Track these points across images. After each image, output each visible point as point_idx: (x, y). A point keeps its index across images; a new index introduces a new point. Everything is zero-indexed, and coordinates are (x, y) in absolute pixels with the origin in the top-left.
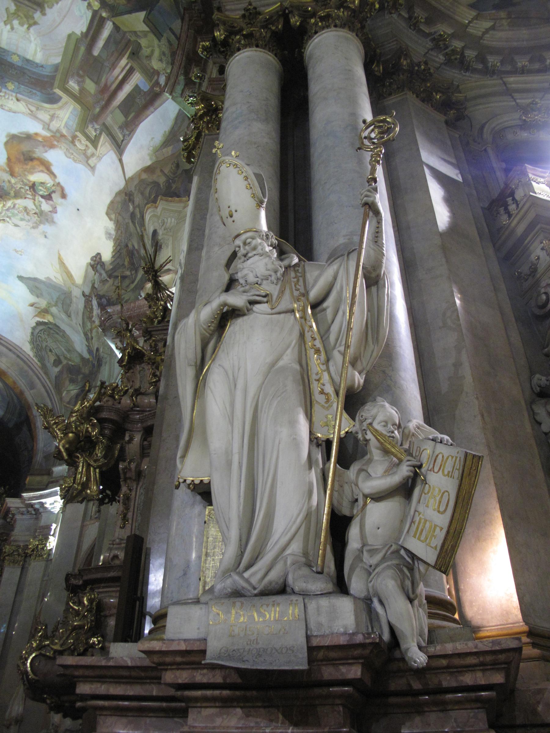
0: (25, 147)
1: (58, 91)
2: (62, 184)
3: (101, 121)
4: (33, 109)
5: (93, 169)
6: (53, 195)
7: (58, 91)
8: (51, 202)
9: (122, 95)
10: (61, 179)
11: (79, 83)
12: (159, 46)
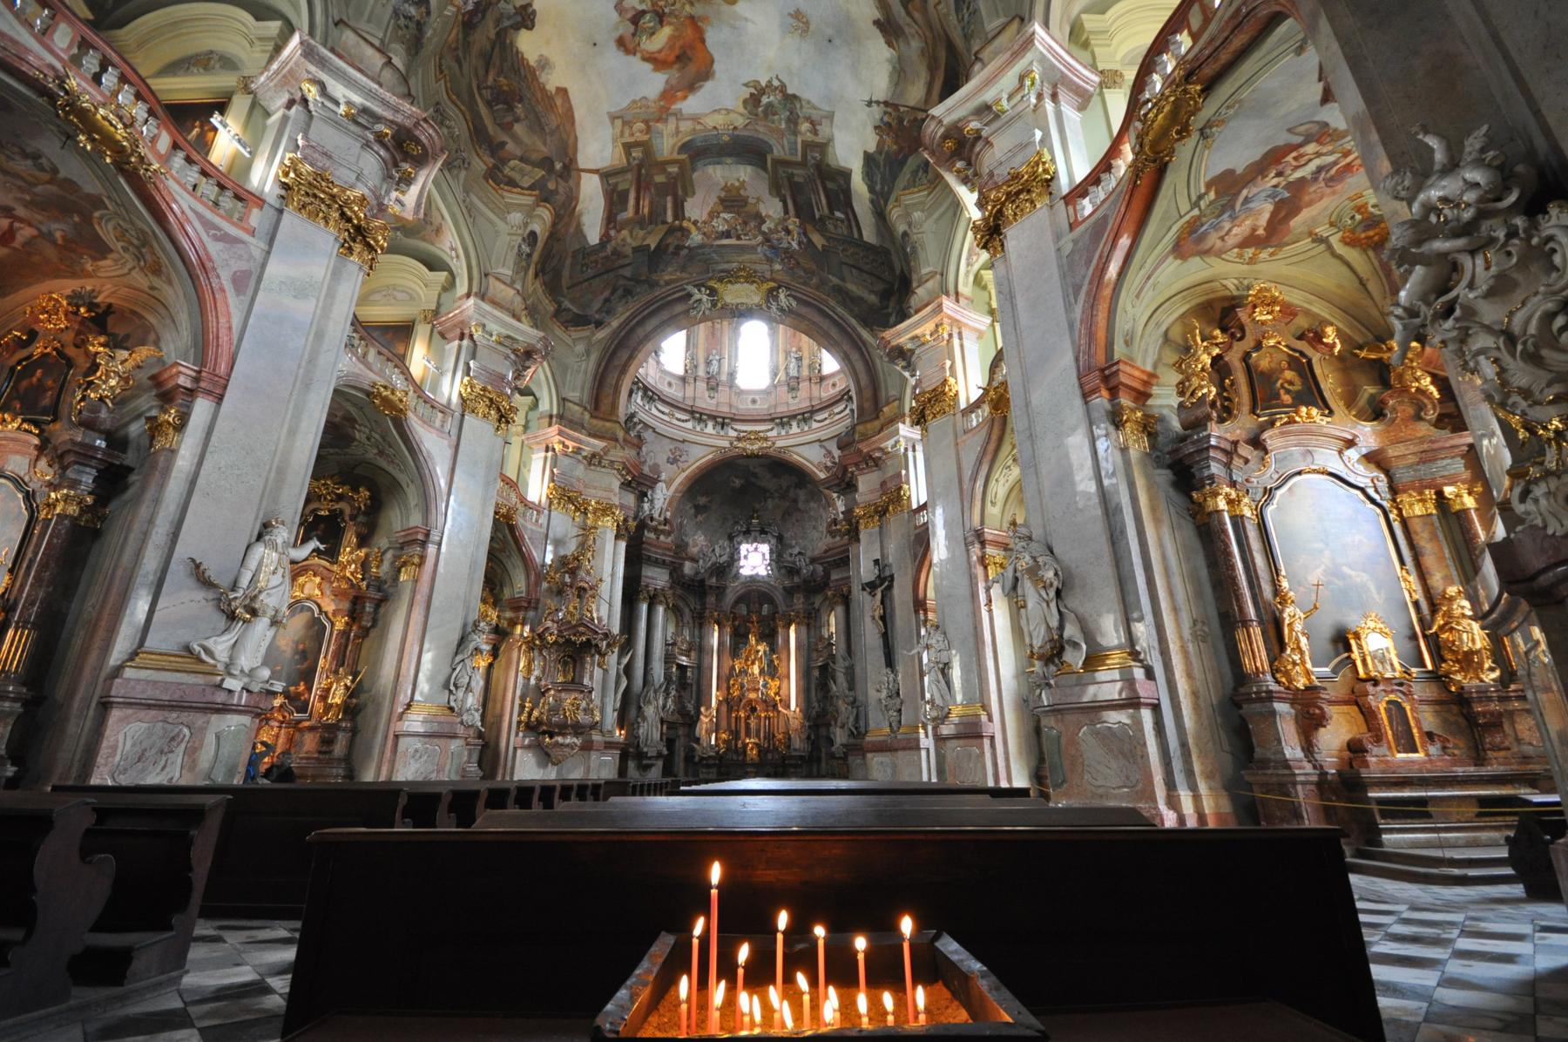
0: (692, 69)
1: (683, 157)
2: (631, 58)
4: (698, 127)
5: (613, 118)
6: (632, 28)
7: (683, 157)
8: (629, 15)
9: (632, 196)
10: (635, 62)
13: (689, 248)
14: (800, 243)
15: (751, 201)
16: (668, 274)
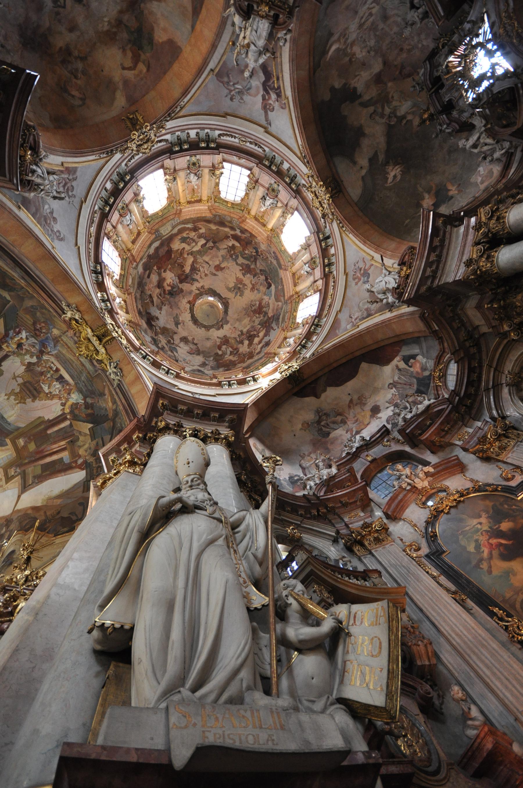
3: (23, 469)
9: (48, 460)
11: (25, 443)
12: (90, 444)
13: (85, 399)
14: (19, 332)
15: (20, 381)
16: (107, 404)
